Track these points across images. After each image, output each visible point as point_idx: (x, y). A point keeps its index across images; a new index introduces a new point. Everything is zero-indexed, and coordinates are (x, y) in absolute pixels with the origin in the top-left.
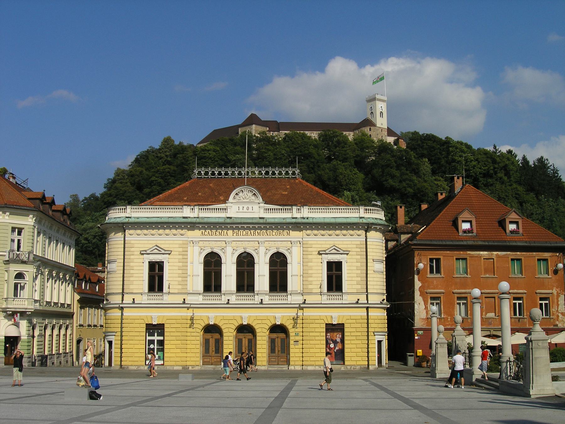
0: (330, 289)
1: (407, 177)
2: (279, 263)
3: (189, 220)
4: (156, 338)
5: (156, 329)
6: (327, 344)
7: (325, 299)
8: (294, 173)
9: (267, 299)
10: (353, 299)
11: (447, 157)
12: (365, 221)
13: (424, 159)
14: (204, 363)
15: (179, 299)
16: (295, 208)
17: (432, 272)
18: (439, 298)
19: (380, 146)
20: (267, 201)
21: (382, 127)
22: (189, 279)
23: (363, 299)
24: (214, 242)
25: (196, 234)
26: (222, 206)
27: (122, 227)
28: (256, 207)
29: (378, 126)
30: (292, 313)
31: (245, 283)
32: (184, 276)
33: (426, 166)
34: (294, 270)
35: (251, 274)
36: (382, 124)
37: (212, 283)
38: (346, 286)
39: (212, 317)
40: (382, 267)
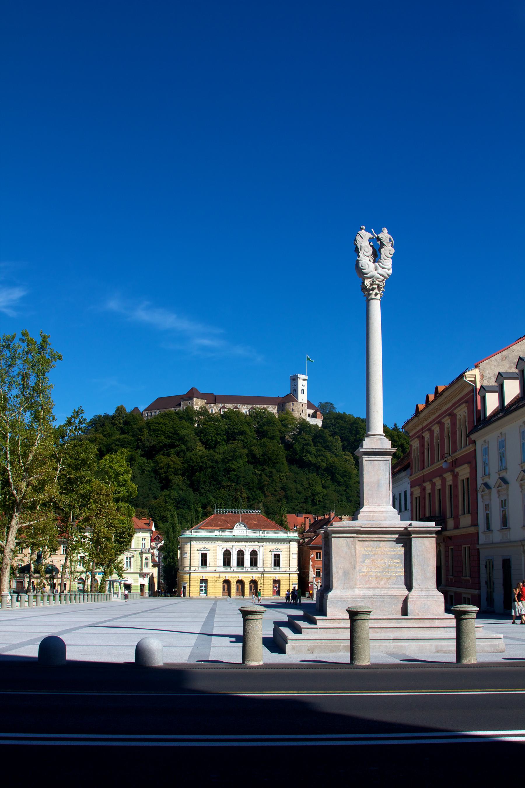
0: (275, 565)
1: (321, 452)
2: (254, 554)
3: (218, 537)
4: (203, 585)
5: (204, 581)
6: (273, 588)
7: (273, 570)
8: (259, 512)
9: (249, 570)
10: (284, 570)
11: (356, 436)
12: (289, 538)
13: (337, 437)
14: (223, 595)
15: (214, 569)
16: (261, 532)
17: (317, 558)
18: (319, 569)
19: (300, 424)
20: (249, 529)
21: (303, 402)
22: (218, 561)
23: (288, 570)
24: (227, 546)
25: (220, 543)
26: (232, 530)
27: (191, 540)
28: (245, 531)
29: (299, 401)
30: (259, 575)
31: (240, 562)
32: (215, 560)
33: (338, 444)
34: (260, 557)
35: (243, 559)
36: (303, 400)
37: (227, 562)
38: (281, 564)
39: (228, 576)
40: (296, 556)
